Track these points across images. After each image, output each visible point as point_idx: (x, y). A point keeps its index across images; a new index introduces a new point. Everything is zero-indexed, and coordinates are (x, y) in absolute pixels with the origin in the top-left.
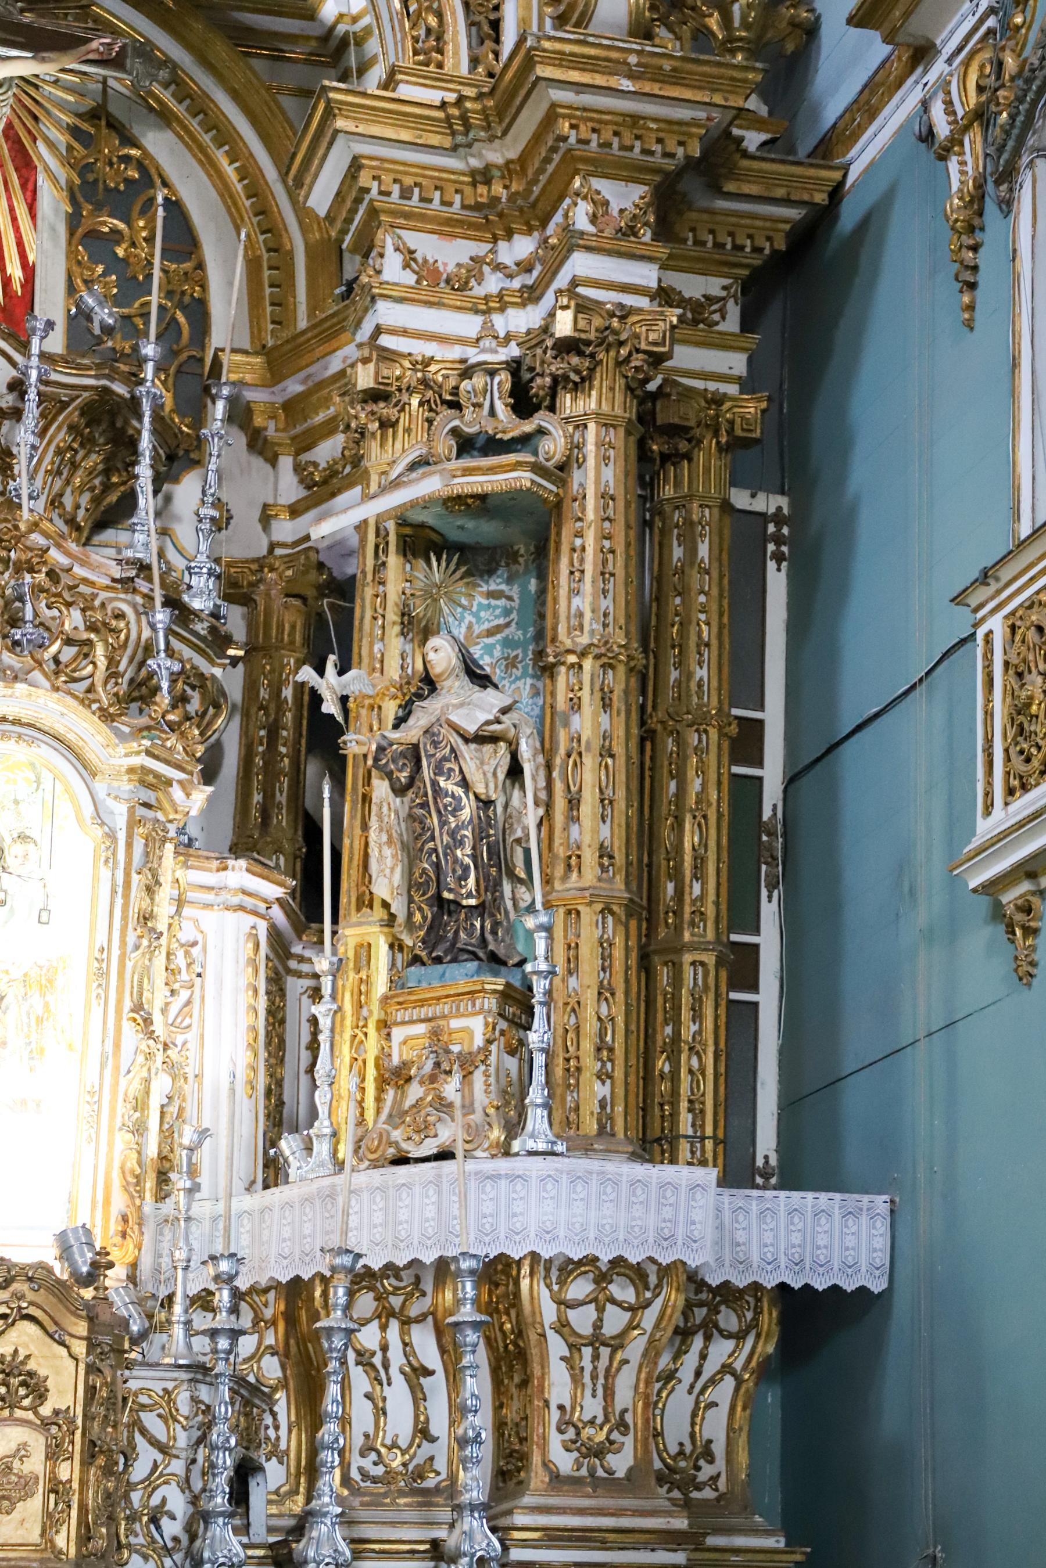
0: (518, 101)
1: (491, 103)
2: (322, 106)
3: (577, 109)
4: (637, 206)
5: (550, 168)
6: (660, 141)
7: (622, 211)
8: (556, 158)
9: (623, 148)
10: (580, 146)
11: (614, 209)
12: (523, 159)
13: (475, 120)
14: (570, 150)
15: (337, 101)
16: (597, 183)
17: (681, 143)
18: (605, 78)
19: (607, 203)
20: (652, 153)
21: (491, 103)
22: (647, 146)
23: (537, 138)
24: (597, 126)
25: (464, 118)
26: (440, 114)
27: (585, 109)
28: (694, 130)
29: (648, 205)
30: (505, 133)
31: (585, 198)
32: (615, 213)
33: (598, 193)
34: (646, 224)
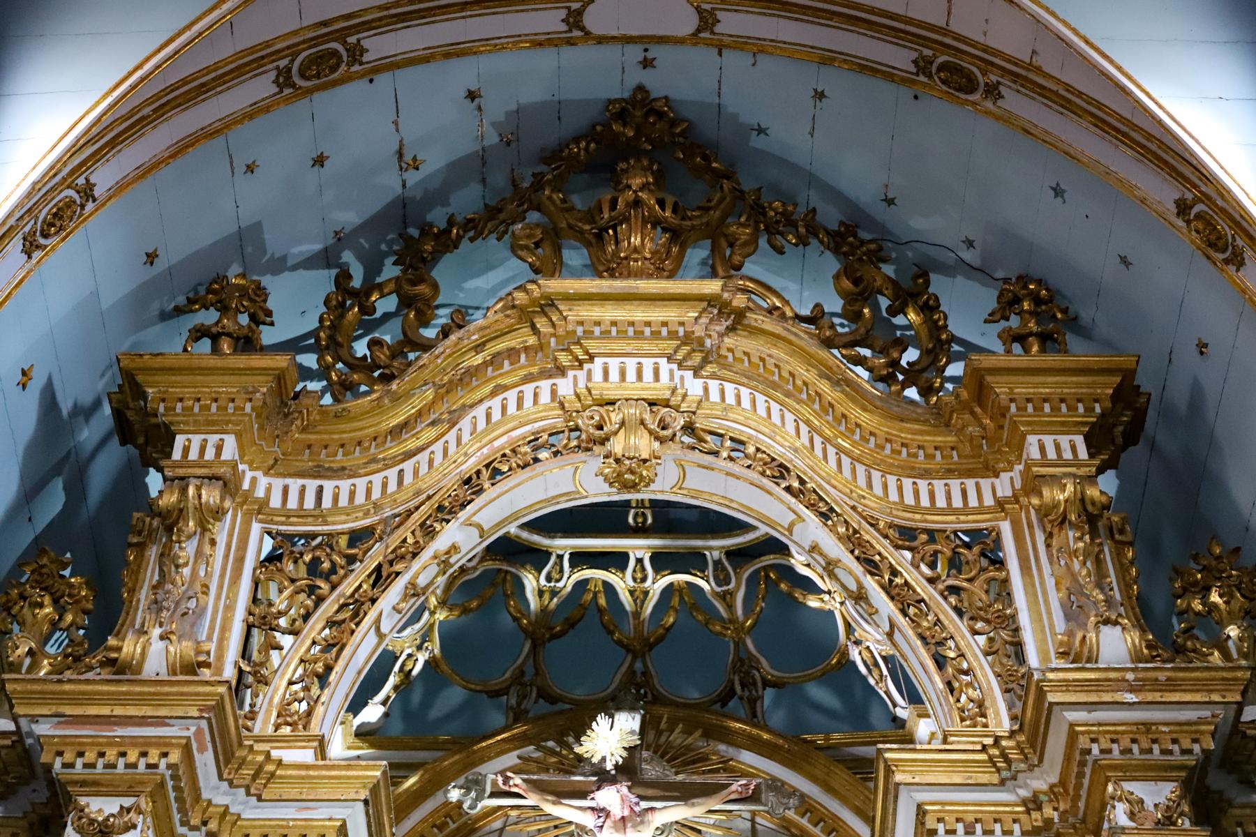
0: (1042, 730)
1: (1023, 738)
2: (882, 766)
3: (1093, 725)
4: (1169, 800)
5: (1086, 782)
6: (1174, 741)
7: (1156, 806)
8: (1088, 770)
9: (1142, 751)
10: (1102, 756)
11: (1149, 804)
12: (1063, 782)
13: (1014, 755)
14: (1096, 761)
15: (892, 760)
16: (1128, 786)
17: (1195, 741)
18: (1110, 694)
19: (1142, 801)
20: (1170, 752)
21: (1023, 738)
22: (1163, 747)
23: (1068, 758)
24: (1114, 737)
25: (1004, 756)
26: (983, 757)
27: (1100, 725)
28: (1203, 728)
29: (1181, 797)
30: (1041, 760)
31: (1120, 800)
32: (1151, 808)
33: (1132, 793)
34: (1182, 814)
